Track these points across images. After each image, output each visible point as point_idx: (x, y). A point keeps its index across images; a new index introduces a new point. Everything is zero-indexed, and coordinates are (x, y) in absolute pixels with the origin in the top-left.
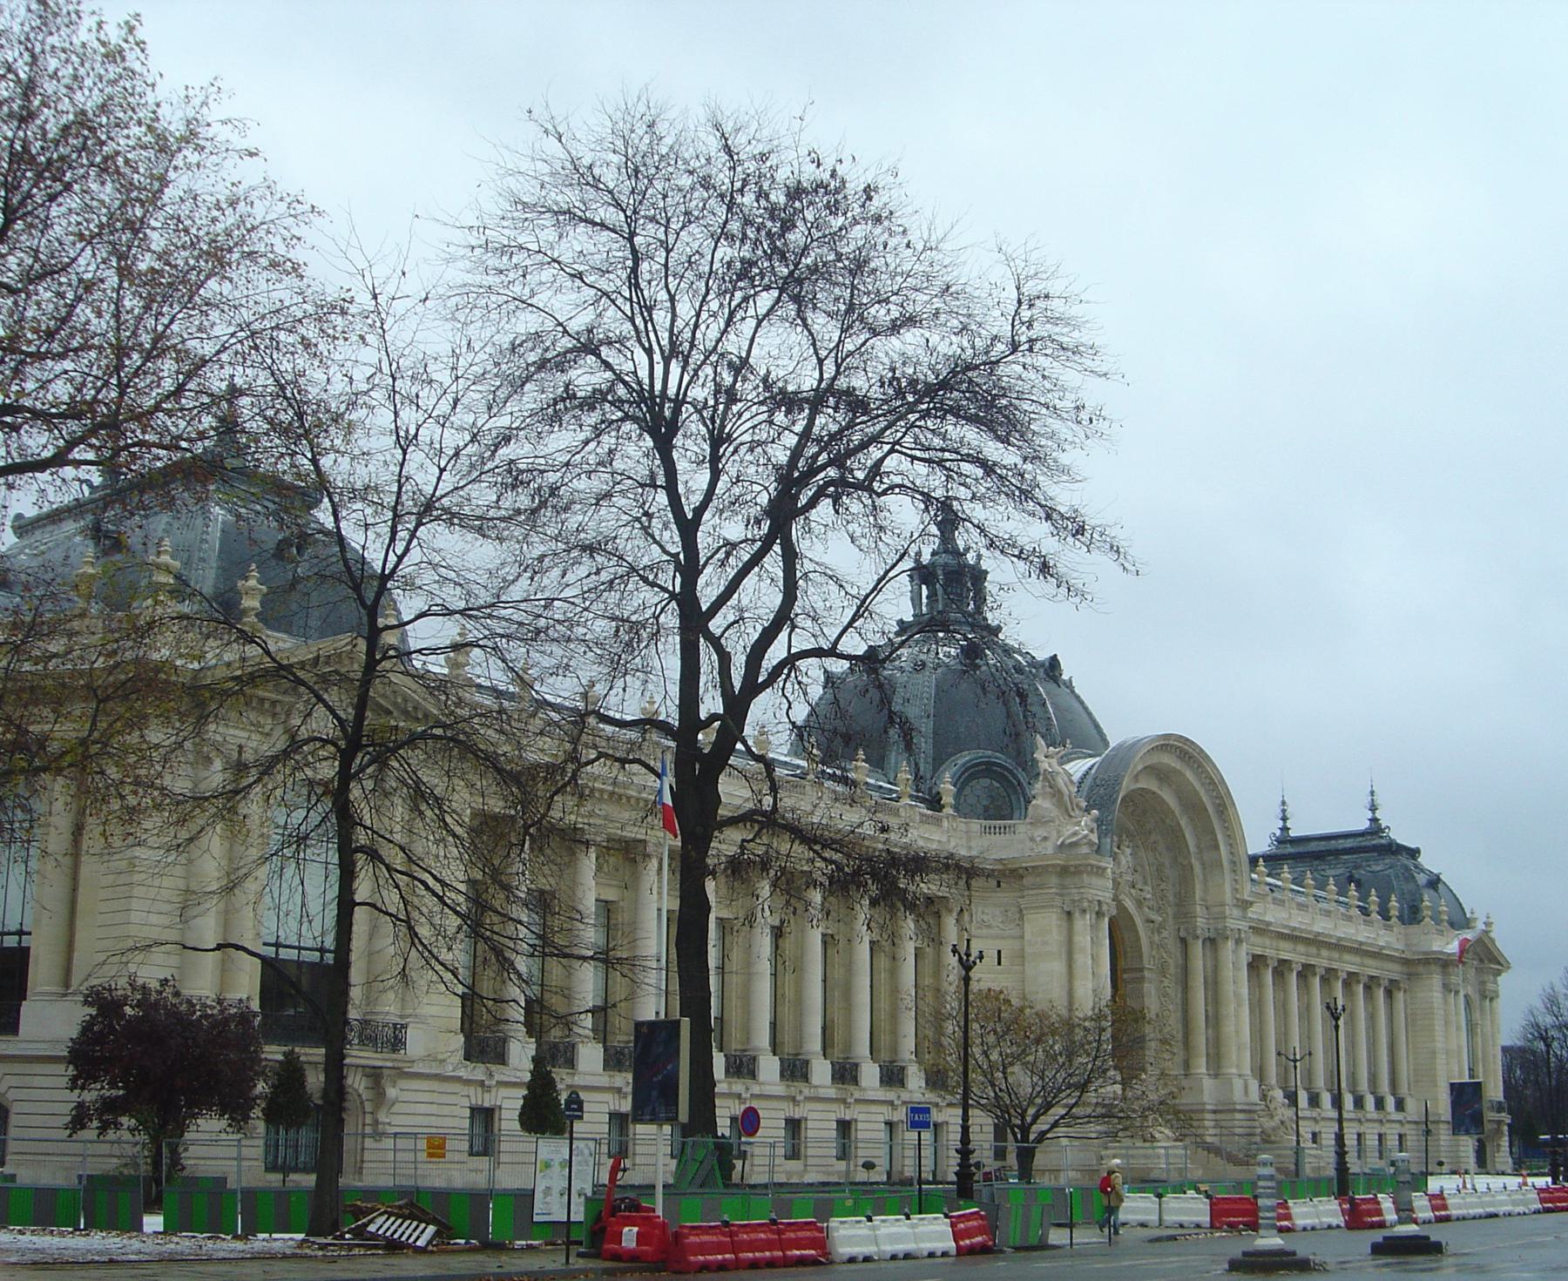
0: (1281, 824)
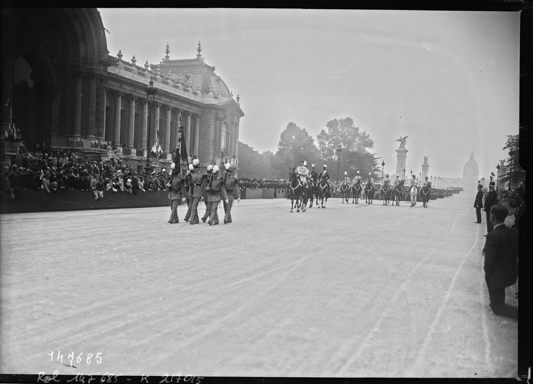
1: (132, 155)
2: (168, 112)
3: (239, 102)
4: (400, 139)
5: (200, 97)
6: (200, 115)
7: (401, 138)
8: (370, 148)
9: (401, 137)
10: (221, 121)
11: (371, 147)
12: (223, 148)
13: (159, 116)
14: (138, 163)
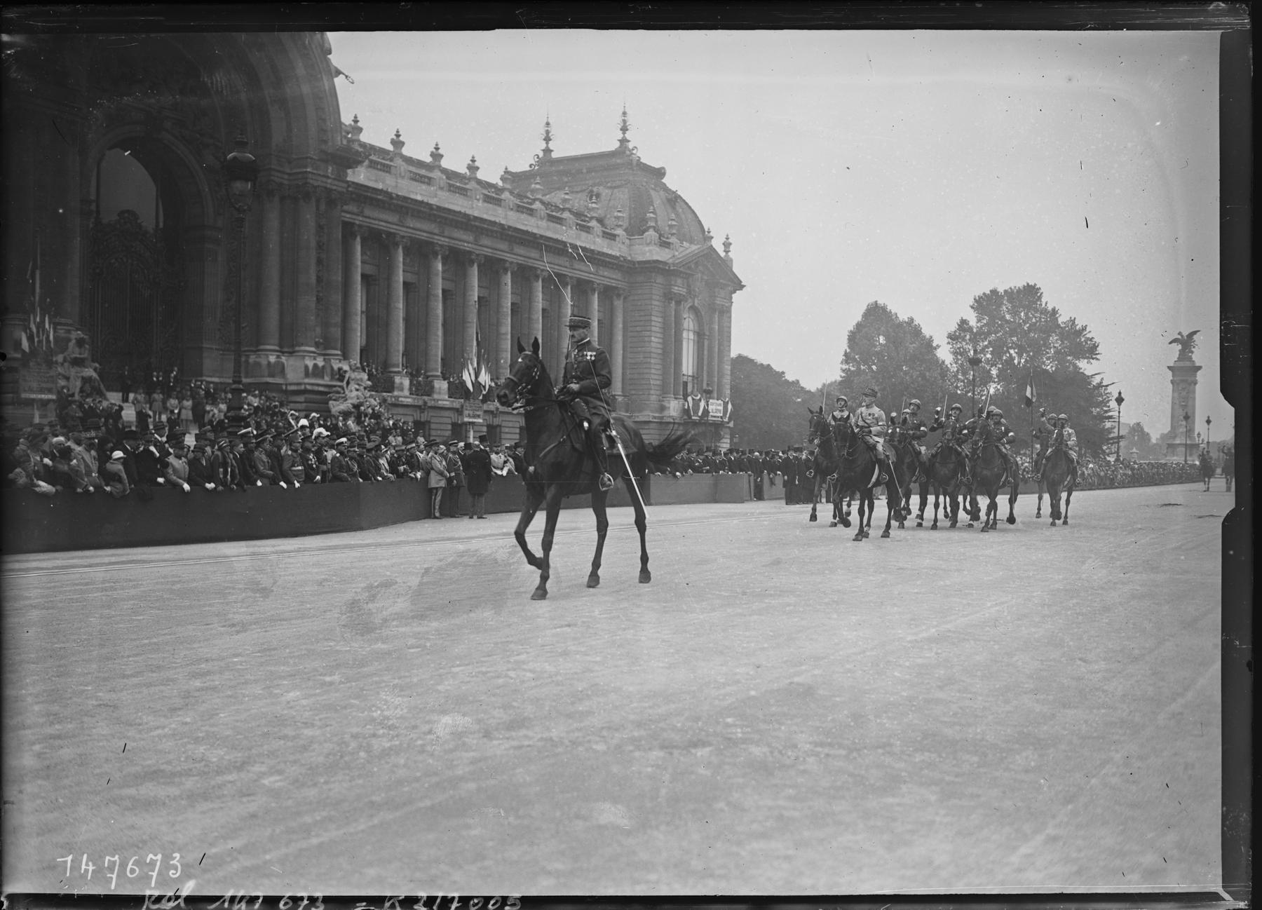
0: (544, 145)
1: (436, 396)
2: (535, 284)
3: (729, 253)
4: (1179, 337)
5: (623, 243)
7: (1182, 336)
8: (1091, 360)
9: (1180, 334)
10: (678, 303)
11: (1093, 359)
12: (690, 374)
13: (510, 296)
14: (452, 416)
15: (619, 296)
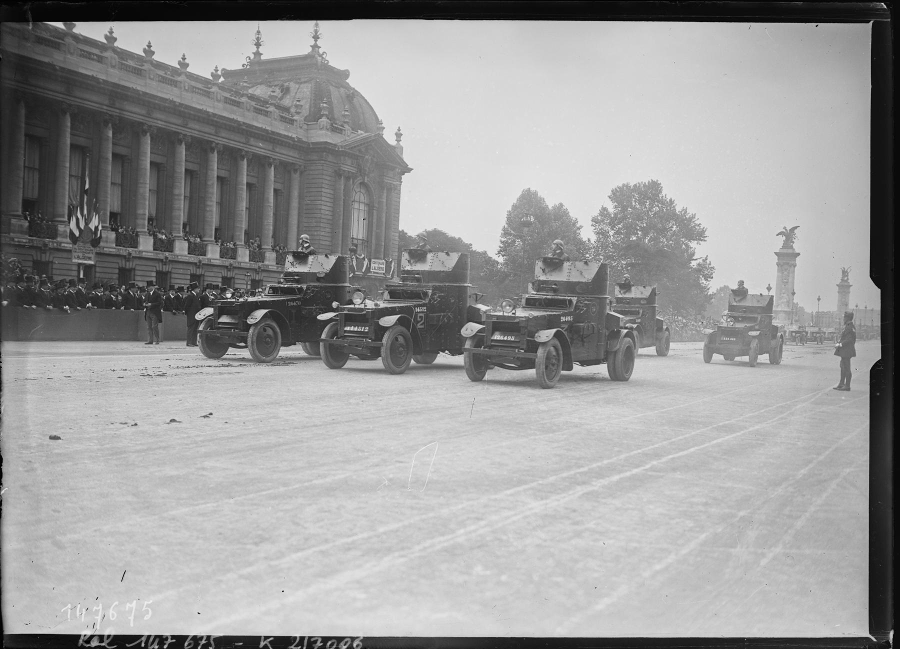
0: (254, 49)
2: (211, 155)
3: (400, 142)
4: (784, 231)
5: (301, 127)
6: (300, 166)
7: (786, 230)
8: (700, 242)
9: (785, 228)
10: (348, 179)
11: (702, 240)
12: (360, 237)
13: (184, 164)
15: (295, 171)
